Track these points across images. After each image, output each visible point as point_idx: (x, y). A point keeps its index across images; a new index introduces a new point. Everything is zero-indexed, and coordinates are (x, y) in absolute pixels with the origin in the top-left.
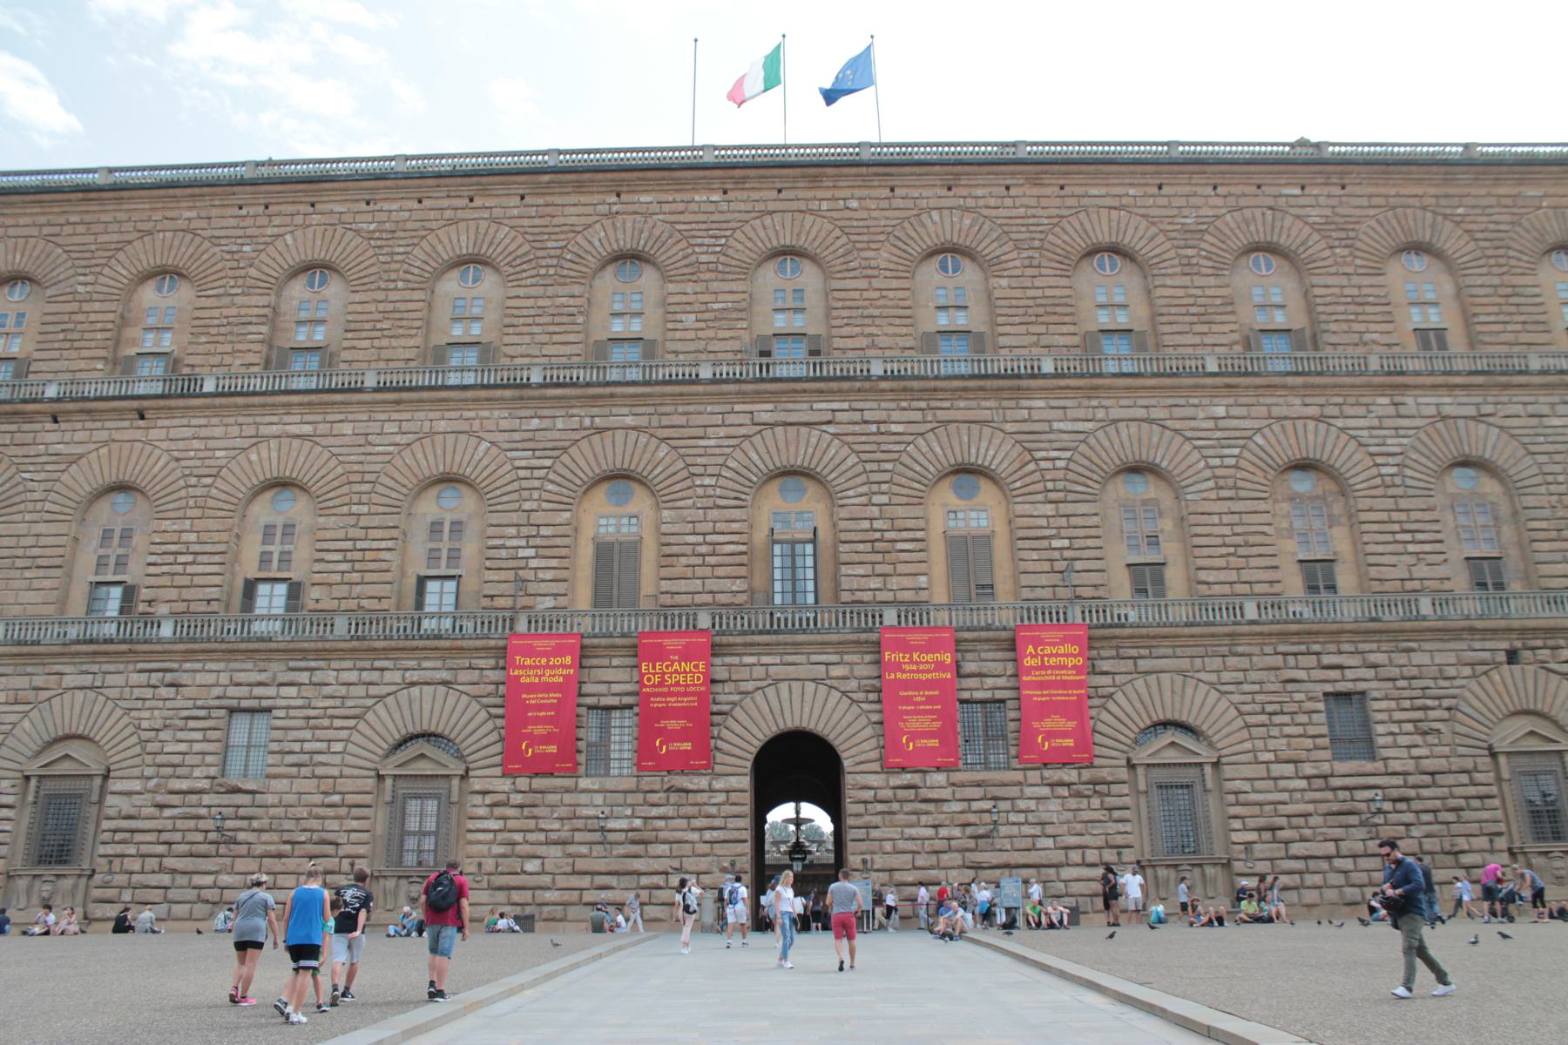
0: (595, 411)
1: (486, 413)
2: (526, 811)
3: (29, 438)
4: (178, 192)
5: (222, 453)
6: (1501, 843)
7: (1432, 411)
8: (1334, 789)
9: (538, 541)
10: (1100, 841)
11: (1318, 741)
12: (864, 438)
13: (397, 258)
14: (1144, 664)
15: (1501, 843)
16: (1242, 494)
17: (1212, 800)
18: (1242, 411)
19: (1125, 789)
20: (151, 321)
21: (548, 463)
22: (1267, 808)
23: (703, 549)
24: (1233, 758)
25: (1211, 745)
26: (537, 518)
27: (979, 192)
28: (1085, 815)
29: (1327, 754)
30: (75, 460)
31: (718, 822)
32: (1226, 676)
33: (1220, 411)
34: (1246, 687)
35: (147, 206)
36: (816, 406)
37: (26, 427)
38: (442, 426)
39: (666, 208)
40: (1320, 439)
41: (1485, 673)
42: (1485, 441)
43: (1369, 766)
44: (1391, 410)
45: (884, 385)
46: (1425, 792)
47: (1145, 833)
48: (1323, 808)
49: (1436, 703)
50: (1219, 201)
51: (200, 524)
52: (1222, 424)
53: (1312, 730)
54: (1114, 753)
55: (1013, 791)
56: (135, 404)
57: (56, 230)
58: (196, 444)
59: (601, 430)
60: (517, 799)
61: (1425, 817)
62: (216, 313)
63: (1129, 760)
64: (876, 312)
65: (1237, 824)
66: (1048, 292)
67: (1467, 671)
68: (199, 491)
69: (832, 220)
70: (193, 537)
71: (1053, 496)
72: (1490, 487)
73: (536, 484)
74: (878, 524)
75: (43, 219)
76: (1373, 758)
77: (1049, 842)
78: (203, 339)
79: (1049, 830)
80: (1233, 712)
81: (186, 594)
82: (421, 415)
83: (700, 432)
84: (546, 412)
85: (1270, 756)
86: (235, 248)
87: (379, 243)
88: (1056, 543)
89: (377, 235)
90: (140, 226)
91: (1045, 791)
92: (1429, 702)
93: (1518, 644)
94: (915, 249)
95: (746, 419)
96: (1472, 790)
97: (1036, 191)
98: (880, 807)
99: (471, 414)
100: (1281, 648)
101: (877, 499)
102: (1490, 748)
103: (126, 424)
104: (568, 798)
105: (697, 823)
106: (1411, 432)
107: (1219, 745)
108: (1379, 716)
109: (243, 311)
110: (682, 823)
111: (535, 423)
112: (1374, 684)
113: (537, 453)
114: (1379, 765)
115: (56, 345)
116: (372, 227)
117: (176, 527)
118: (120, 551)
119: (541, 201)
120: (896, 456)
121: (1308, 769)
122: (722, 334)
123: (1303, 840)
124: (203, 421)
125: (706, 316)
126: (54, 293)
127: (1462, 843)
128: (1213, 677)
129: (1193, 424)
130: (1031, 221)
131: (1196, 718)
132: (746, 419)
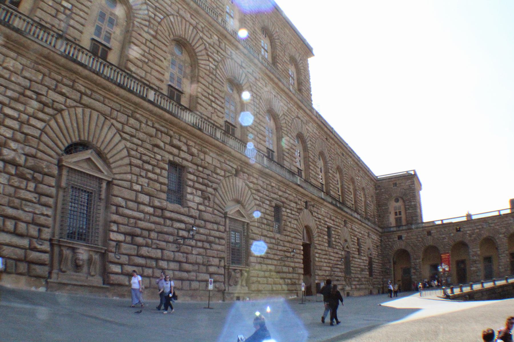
6: (222, 264)
8: (165, 218)
10: (29, 218)
11: (163, 187)
14: (86, 100)
16: (158, 37)
17: (102, 205)
19: (52, 181)
22: (132, 221)
24: (120, 182)
28: (23, 194)
32: (127, 129)
34: (135, 140)
40: (193, 35)
47: (58, 218)
53: (162, 180)
54: (53, 153)
63: (60, 161)
65: (114, 227)
67: (222, 173)
76: (182, 205)
80: (125, 153)
85: (138, 187)
96: (217, 234)
102: (226, 214)
107: (114, 171)
108: (190, 183)
112: (190, 165)
114: (186, 209)
121: (157, 203)
123: (147, 245)
128: (119, 126)
131: (105, 148)
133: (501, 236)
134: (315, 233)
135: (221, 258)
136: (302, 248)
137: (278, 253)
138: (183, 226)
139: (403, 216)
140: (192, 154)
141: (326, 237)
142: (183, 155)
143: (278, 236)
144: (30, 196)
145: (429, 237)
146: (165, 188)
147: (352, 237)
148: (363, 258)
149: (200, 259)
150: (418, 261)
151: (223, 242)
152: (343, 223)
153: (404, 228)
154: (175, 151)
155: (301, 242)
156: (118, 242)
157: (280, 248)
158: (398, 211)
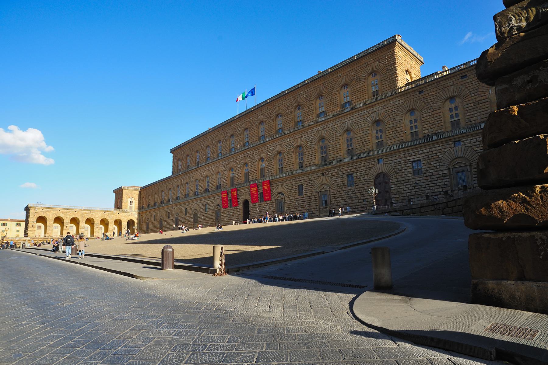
6: (318, 207)
7: (317, 130)
15: (318, 207)
18: (291, 139)
25: (283, 195)
30: (193, 177)
32: (286, 185)
33: (288, 140)
41: (318, 178)
43: (301, 196)
46: (308, 200)
49: (311, 185)
59: (229, 162)
61: (308, 204)
65: (286, 207)
91: (267, 204)
92: (310, 185)
93: (323, 172)
106: (313, 136)
127: (312, 208)
129: (285, 143)
138: (302, 201)
149: (308, 208)
154: (298, 182)
156: (287, 210)
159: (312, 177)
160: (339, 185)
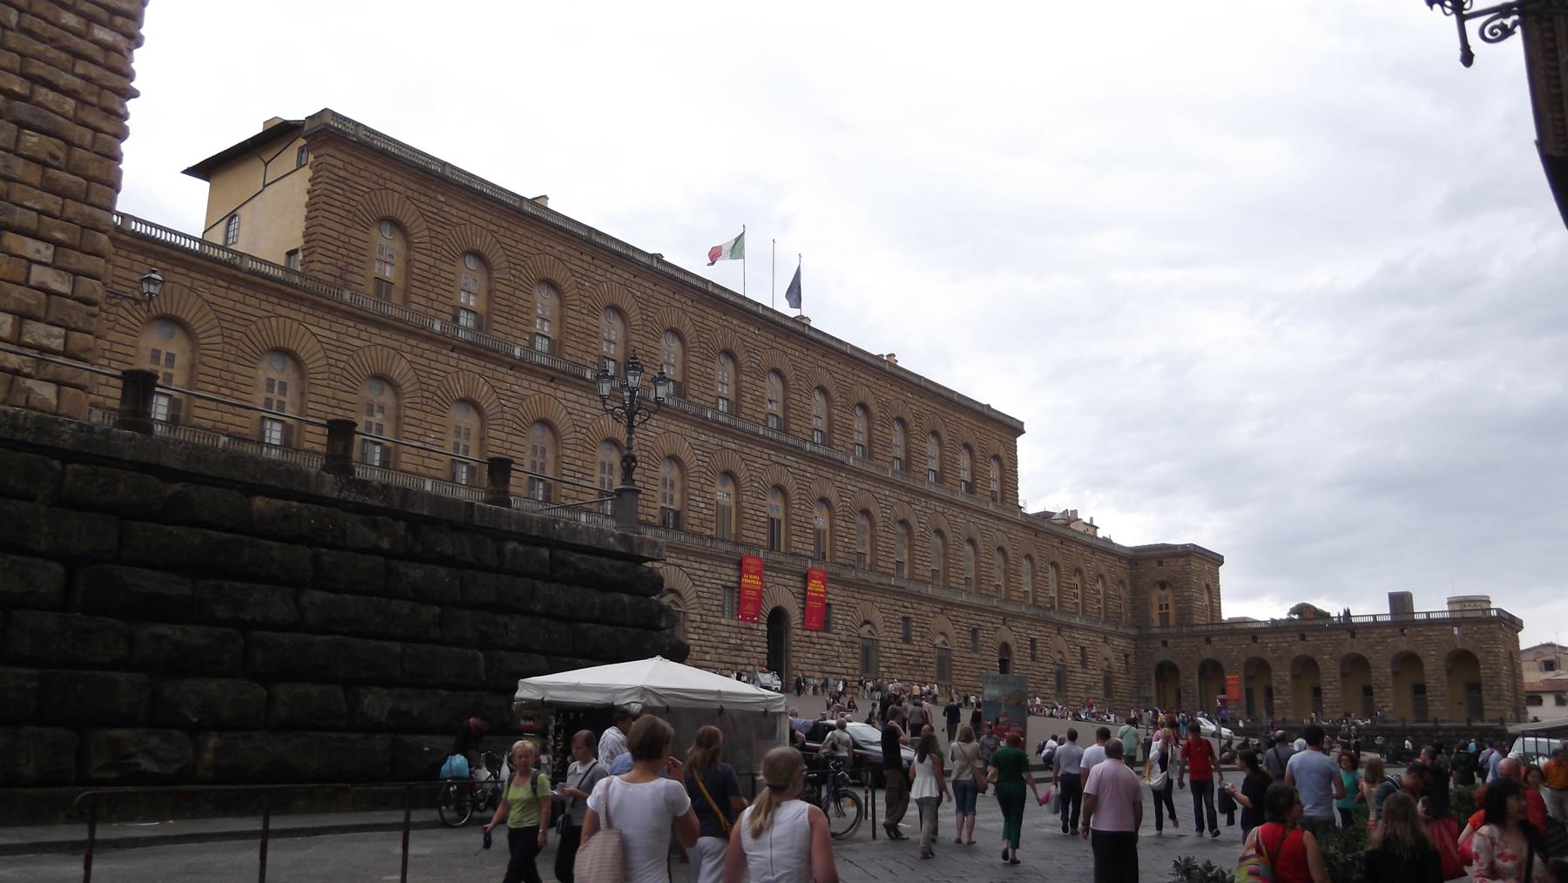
0: (722, 437)
1: (686, 426)
2: (706, 632)
3: (500, 376)
4: (561, 233)
5: (588, 416)
8: (902, 654)
9: (706, 500)
12: (799, 477)
13: (649, 319)
14: (865, 597)
20: (539, 311)
21: (708, 460)
23: (755, 518)
26: (706, 488)
27: (832, 363)
29: (901, 641)
30: (523, 398)
31: (760, 644)
32: (883, 606)
33: (887, 493)
35: (540, 232)
36: (788, 457)
37: (499, 368)
38: (672, 428)
39: (742, 330)
42: (944, 526)
43: (912, 647)
44: (924, 504)
45: (809, 455)
48: (899, 661)
50: (891, 393)
51: (584, 456)
52: (889, 499)
55: (831, 642)
56: (556, 374)
57: (496, 228)
58: (578, 406)
60: (704, 626)
62: (576, 322)
64: (802, 414)
66: (848, 422)
68: (581, 436)
69: (790, 359)
70: (580, 463)
71: (846, 518)
72: (939, 542)
73: (704, 470)
74: (803, 519)
75: (488, 217)
77: (839, 665)
78: (573, 338)
79: (841, 659)
81: (582, 496)
82: (664, 419)
83: (753, 459)
84: (706, 432)
85: (889, 639)
86: (582, 282)
87: (641, 306)
88: (846, 540)
89: (641, 300)
90: (539, 246)
91: (838, 643)
94: (814, 386)
95: (765, 456)
97: (846, 368)
98: (801, 644)
99: (681, 425)
100: (896, 597)
101: (803, 507)
103: (546, 383)
104: (718, 627)
105: (755, 644)
109: (590, 327)
110: (748, 643)
111: (703, 437)
112: (913, 616)
113: (705, 454)
115: (505, 315)
116: (639, 294)
117: (572, 455)
118: (542, 460)
119: (700, 307)
120: (807, 488)
122: (759, 409)
124: (580, 393)
125: (754, 397)
126: (499, 276)
128: (878, 605)
130: (846, 384)
132: (765, 456)
133: (1325, 657)
134: (1014, 648)
135: (932, 677)
136: (998, 664)
137: (975, 670)
138: (910, 658)
139: (1172, 610)
140: (913, 609)
141: (1029, 651)
142: (910, 611)
143: (975, 655)
144: (850, 655)
145: (1208, 646)
146: (901, 636)
147: (1071, 647)
148: (1090, 672)
150: (1191, 680)
151: (933, 665)
152: (1056, 632)
153: (1173, 630)
154: (905, 610)
155: (997, 659)
157: (976, 666)
158: (1164, 603)
159: (926, 608)
160: (963, 645)
